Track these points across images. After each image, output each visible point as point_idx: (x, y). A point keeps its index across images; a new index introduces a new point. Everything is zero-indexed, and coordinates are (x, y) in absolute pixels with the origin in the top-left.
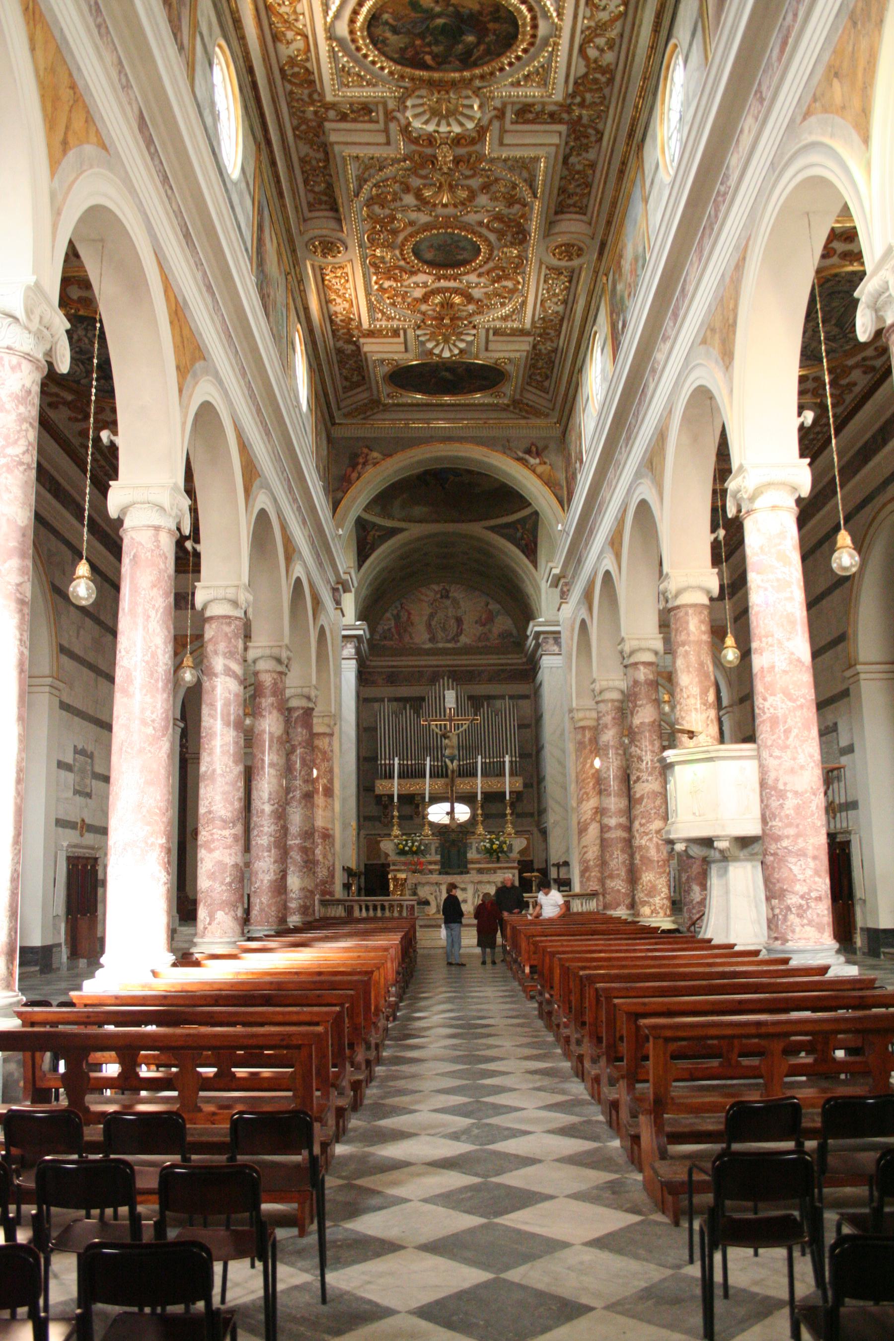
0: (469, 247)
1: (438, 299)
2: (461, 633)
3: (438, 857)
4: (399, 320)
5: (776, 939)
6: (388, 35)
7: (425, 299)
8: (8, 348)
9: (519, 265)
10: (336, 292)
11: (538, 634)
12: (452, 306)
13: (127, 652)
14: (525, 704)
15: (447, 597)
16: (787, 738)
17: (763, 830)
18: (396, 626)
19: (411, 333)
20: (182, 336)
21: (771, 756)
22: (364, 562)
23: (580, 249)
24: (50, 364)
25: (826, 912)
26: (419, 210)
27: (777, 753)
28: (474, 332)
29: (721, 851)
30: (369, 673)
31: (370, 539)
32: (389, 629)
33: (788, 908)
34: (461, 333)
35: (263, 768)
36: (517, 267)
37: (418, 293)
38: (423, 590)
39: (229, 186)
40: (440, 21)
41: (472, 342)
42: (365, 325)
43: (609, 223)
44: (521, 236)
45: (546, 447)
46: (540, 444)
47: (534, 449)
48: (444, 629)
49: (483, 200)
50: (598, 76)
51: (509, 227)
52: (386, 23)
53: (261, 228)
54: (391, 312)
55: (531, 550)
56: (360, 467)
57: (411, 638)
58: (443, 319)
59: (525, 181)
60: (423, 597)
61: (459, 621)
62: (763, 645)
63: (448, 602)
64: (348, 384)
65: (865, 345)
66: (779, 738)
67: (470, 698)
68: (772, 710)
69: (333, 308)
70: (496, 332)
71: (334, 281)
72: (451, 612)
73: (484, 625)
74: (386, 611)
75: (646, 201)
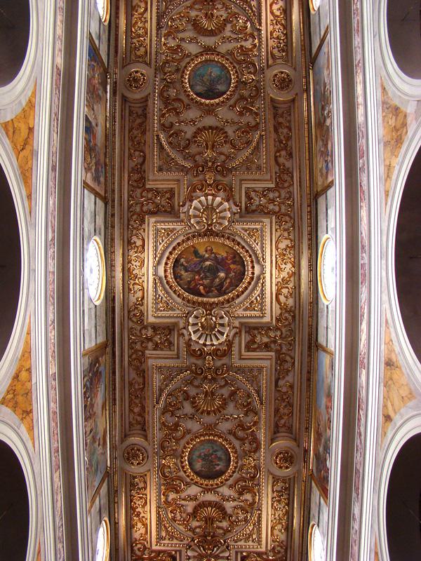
6: (183, 272)
40: (208, 263)
50: (287, 315)
52: (182, 265)
58: (206, 537)
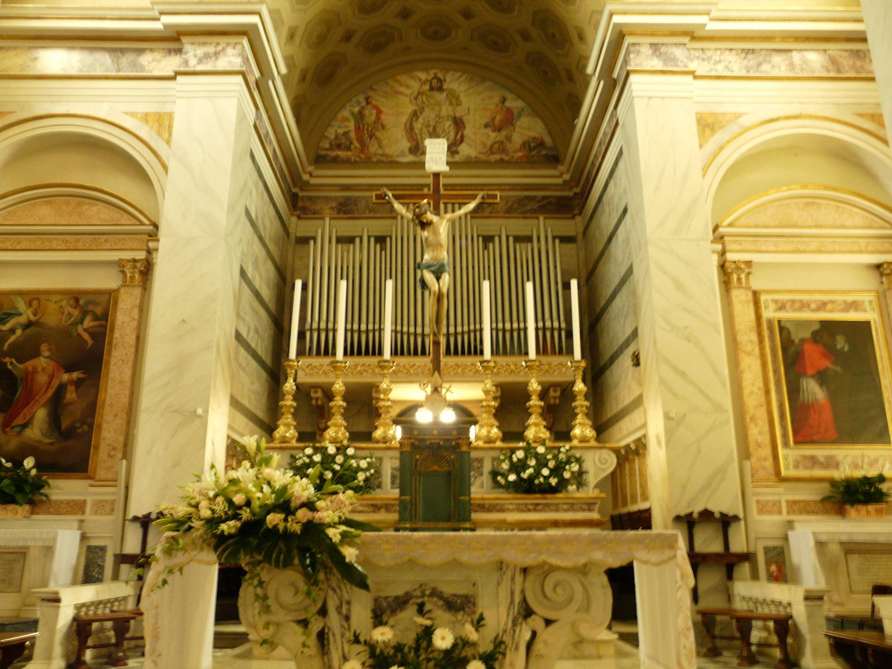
2: (462, 140)
15: (440, 89)
18: (358, 129)
30: (310, 198)
32: (346, 134)
38: (403, 78)
57: (380, 147)
60: (403, 89)
72: (446, 110)
73: (499, 129)
74: (343, 107)
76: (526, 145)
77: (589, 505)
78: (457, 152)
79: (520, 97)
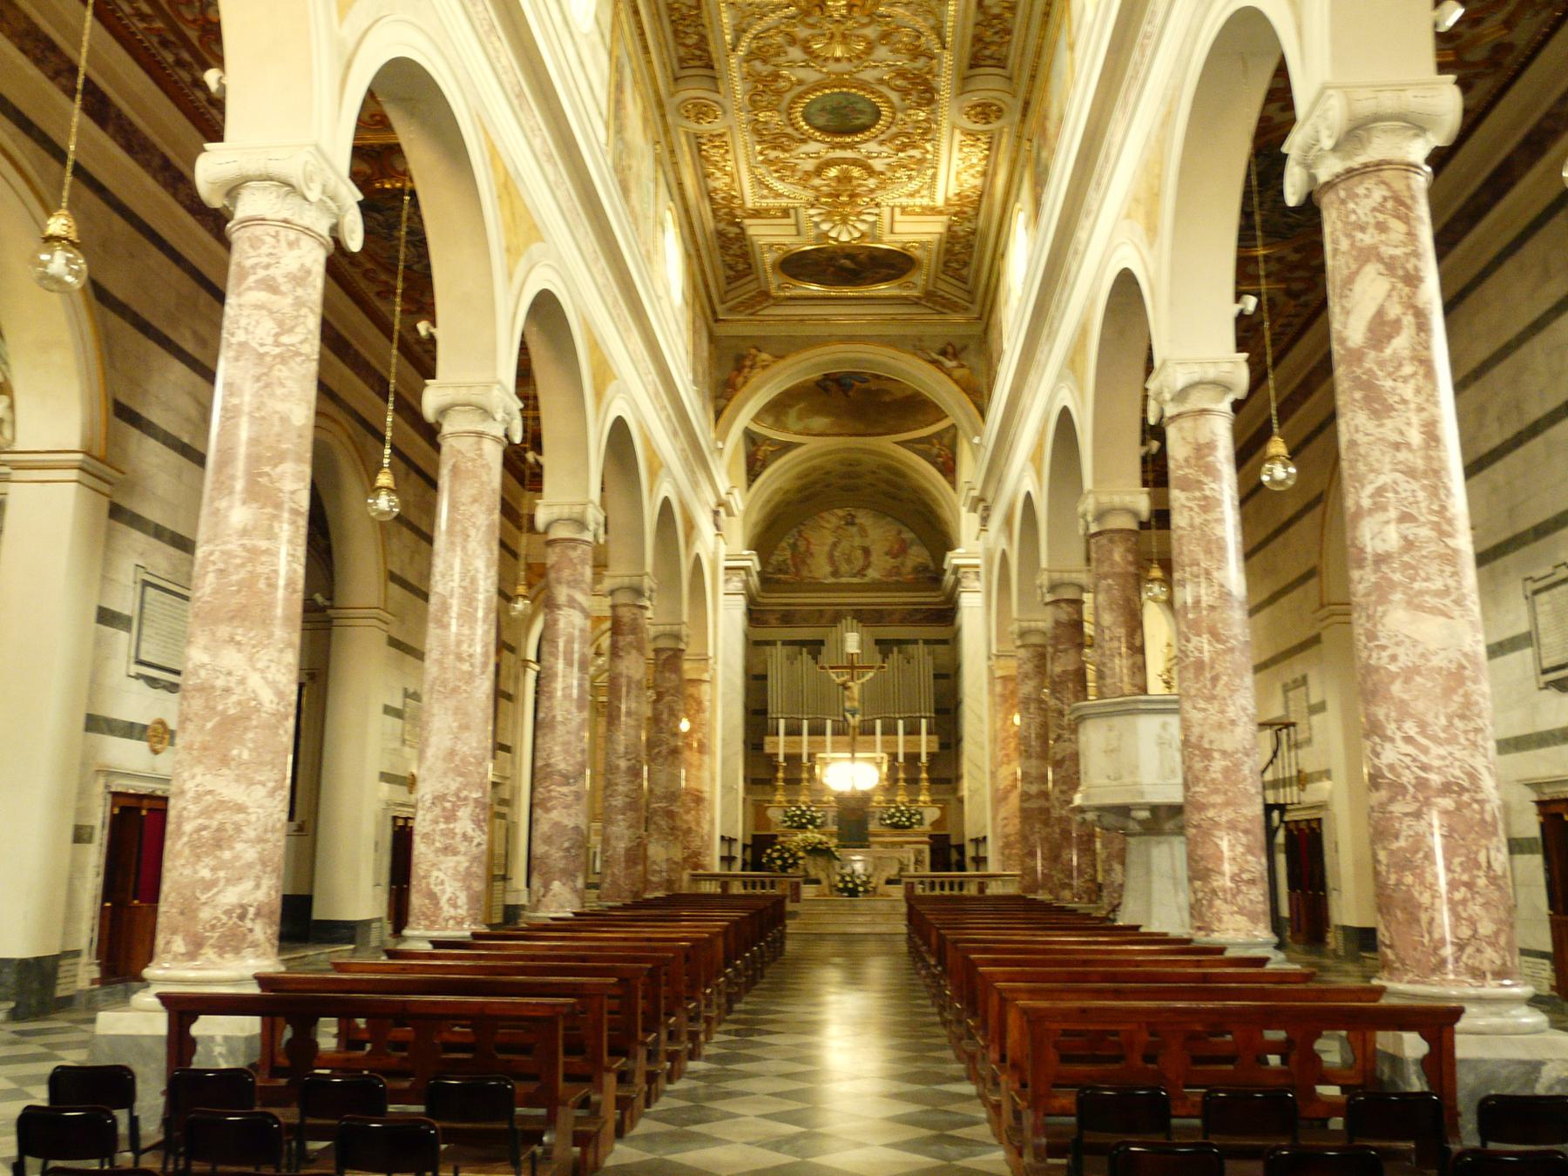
0: (869, 110)
1: (833, 172)
3: (835, 828)
4: (788, 197)
5: (1200, 928)
7: (818, 172)
8: (285, 221)
9: (927, 132)
10: (715, 164)
11: (957, 568)
12: (849, 179)
13: (443, 576)
14: (940, 648)
15: (853, 524)
16: (1214, 686)
17: (1185, 797)
18: (793, 555)
19: (802, 210)
20: (513, 214)
21: (1195, 708)
22: (753, 481)
23: (1000, 110)
24: (337, 242)
25: (1261, 898)
26: (808, 66)
27: (1202, 704)
28: (876, 211)
29: (1141, 822)
31: (760, 455)
32: (784, 561)
33: (1214, 892)
34: (860, 213)
35: (619, 717)
36: (926, 131)
37: (810, 165)
38: (825, 514)
39: (577, 38)
41: (874, 224)
42: (749, 205)
43: (1033, 77)
44: (928, 95)
45: (965, 348)
46: (958, 346)
47: (950, 350)
48: (849, 561)
49: (882, 52)
51: (913, 84)
53: (619, 87)
54: (780, 187)
55: (948, 468)
56: (746, 370)
58: (838, 196)
59: (933, 28)
61: (866, 552)
62: (1187, 575)
63: (854, 529)
64: (731, 273)
65: (1293, 209)
66: (1205, 686)
67: (878, 642)
68: (1197, 654)
69: (713, 184)
70: (904, 210)
71: (712, 151)
72: (857, 541)
73: (895, 557)
74: (781, 540)
75: (1072, 47)
76: (916, 570)
77: (923, 834)
78: (864, 575)
79: (912, 530)
